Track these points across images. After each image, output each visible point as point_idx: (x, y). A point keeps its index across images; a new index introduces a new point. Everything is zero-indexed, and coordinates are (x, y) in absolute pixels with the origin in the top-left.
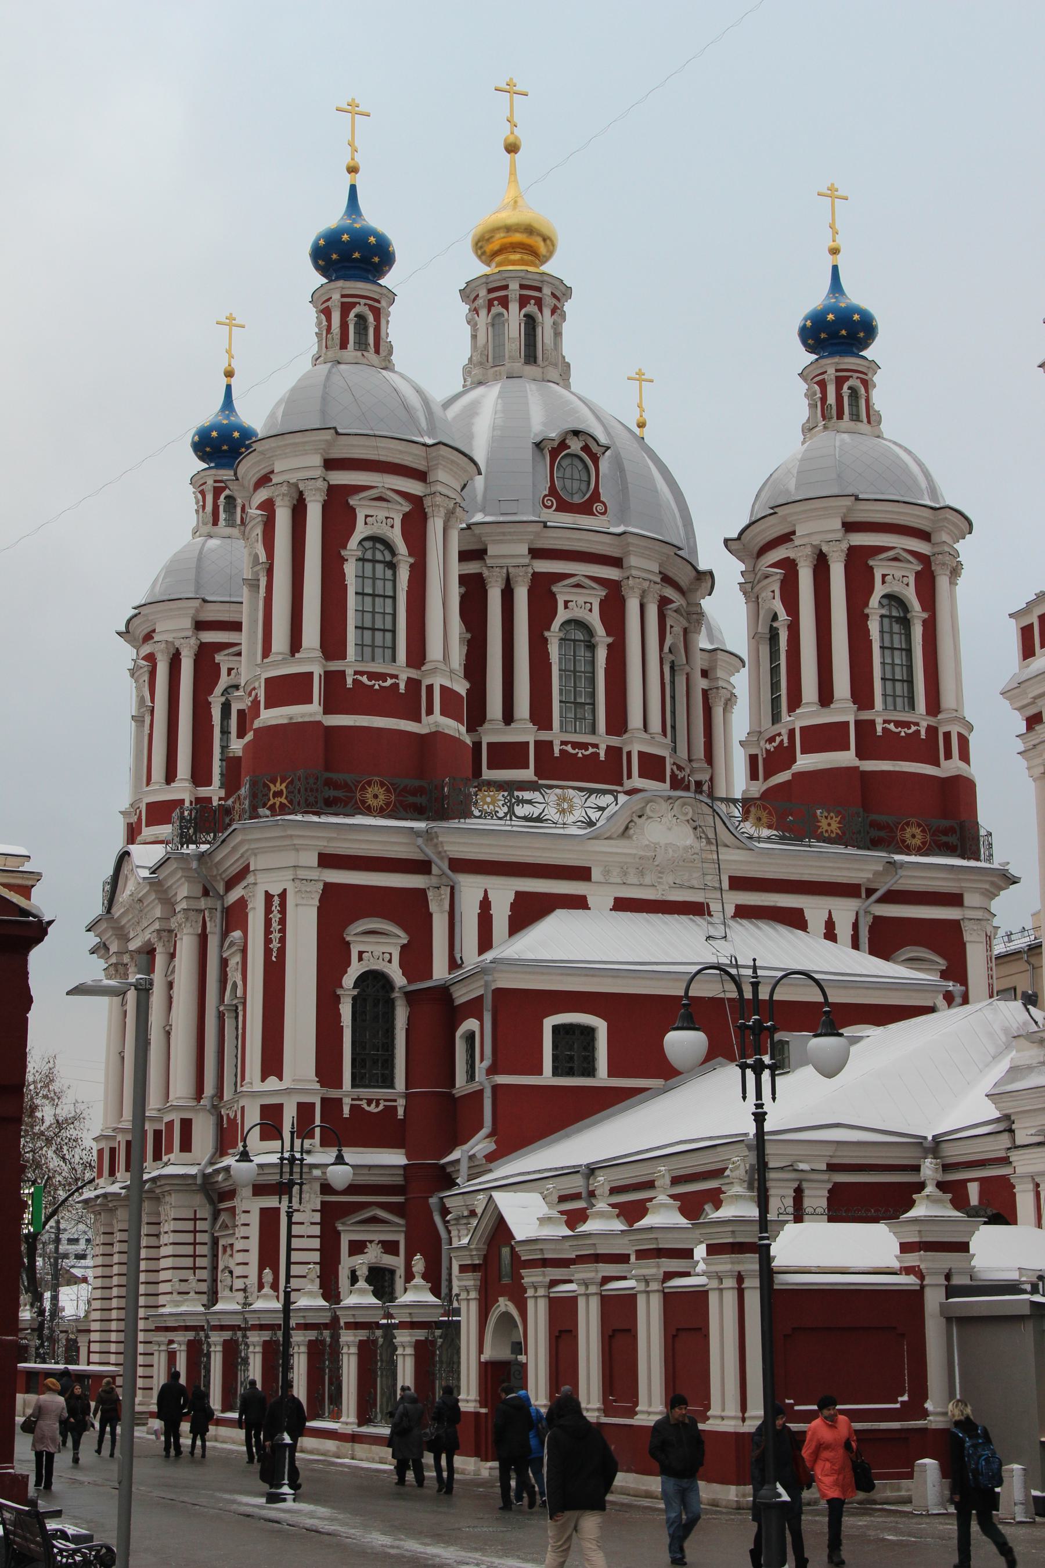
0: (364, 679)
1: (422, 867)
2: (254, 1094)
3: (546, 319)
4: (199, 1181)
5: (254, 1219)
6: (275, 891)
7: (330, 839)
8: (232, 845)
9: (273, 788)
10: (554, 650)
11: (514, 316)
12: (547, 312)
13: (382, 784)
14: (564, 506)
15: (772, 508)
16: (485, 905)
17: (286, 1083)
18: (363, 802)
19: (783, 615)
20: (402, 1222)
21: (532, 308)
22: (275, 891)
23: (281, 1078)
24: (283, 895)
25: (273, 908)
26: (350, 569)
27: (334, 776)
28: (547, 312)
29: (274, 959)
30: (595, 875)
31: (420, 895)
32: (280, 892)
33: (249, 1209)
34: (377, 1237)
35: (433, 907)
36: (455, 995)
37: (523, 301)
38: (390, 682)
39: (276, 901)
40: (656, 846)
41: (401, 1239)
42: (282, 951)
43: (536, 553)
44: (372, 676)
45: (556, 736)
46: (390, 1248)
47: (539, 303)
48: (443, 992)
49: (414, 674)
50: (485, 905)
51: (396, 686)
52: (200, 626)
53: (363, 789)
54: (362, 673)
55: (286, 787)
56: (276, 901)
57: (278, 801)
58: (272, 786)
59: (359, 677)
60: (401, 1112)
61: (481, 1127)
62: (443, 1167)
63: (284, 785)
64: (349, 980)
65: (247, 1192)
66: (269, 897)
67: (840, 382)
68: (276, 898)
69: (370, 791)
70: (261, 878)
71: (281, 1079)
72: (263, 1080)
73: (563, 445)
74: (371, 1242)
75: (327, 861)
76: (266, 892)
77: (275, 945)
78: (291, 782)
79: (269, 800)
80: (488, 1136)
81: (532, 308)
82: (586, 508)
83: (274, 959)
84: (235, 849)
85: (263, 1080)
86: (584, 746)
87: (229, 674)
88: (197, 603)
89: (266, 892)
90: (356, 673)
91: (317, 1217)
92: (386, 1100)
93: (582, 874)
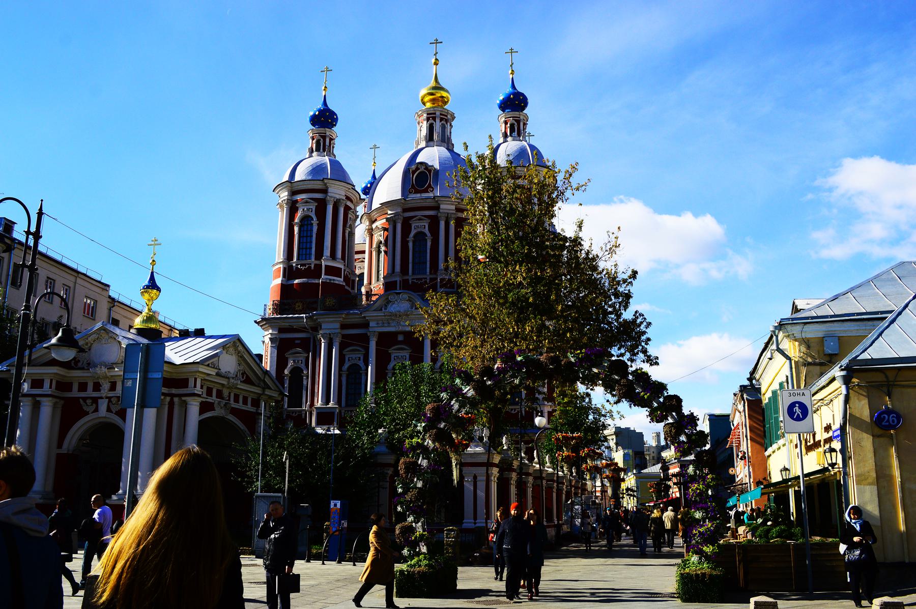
3: (438, 126)
10: (411, 245)
11: (425, 125)
12: (438, 120)
14: (417, 192)
21: (431, 121)
28: (438, 120)
37: (428, 119)
43: (405, 210)
45: (410, 277)
47: (434, 119)
49: (318, 262)
73: (417, 169)
81: (430, 121)
82: (426, 191)
86: (421, 279)
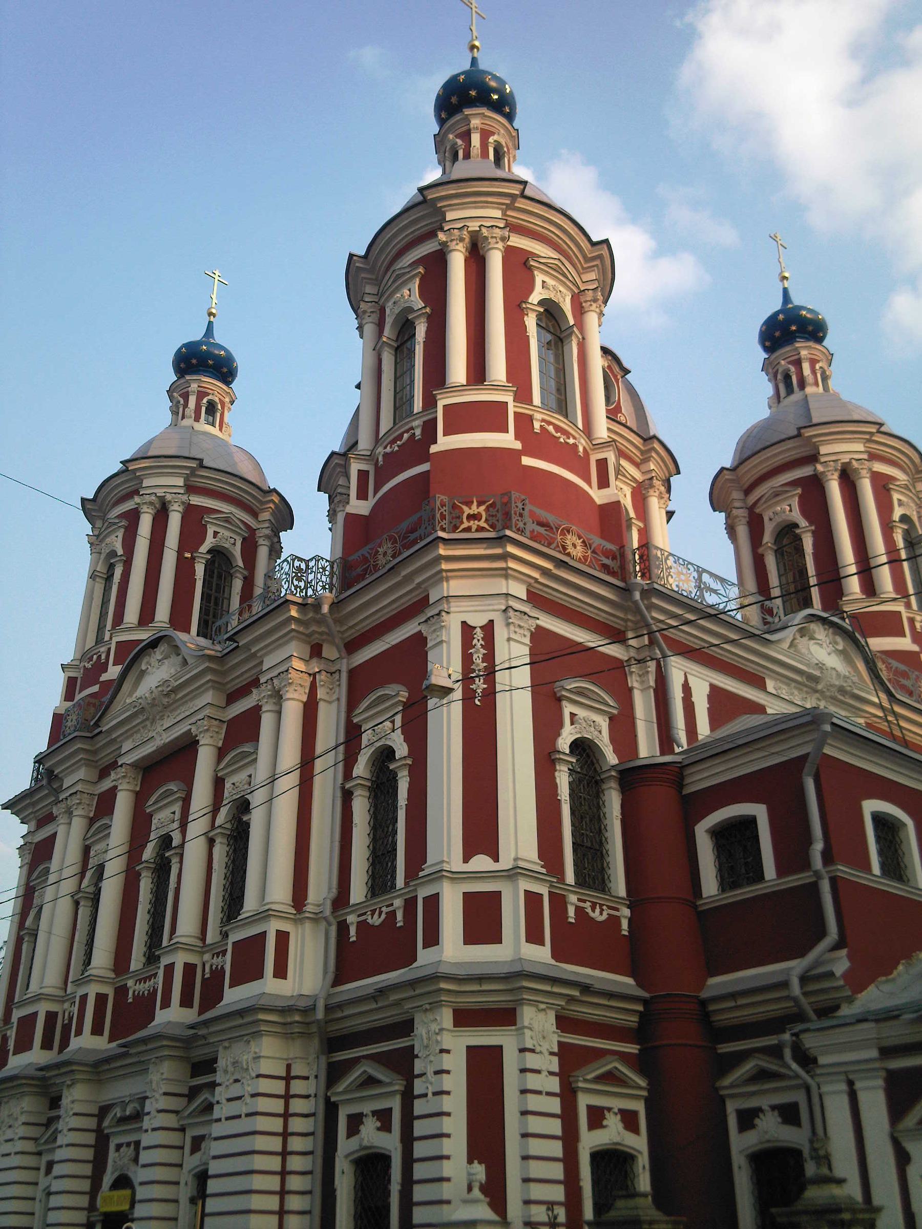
0: (551, 428)
1: (618, 637)
2: (457, 877)
4: (320, 1014)
5: (456, 1064)
6: (477, 620)
7: (545, 572)
8: (404, 573)
9: (467, 511)
13: (580, 537)
15: (799, 429)
16: (687, 689)
17: (506, 862)
18: (564, 548)
19: (803, 523)
20: (642, 1083)
22: (477, 620)
23: (496, 859)
24: (489, 628)
25: (475, 641)
26: (531, 322)
27: (538, 511)
29: (478, 703)
30: (770, 685)
31: (619, 667)
32: (484, 622)
33: (446, 1051)
34: (617, 1104)
35: (633, 681)
36: (688, 780)
38: (571, 441)
39: (479, 634)
40: (820, 666)
41: (639, 1107)
42: (490, 694)
44: (558, 428)
46: (629, 1120)
48: (672, 775)
50: (687, 689)
51: (575, 446)
52: (191, 489)
53: (563, 534)
54: (549, 423)
55: (487, 510)
56: (479, 634)
57: (474, 524)
58: (465, 508)
59: (546, 426)
60: (625, 924)
61: (822, 933)
62: (703, 1003)
63: (482, 508)
64: (564, 742)
65: (446, 1017)
66: (467, 629)
67: (813, 362)
68: (478, 630)
69: (570, 539)
70: (454, 606)
71: (496, 859)
72: (466, 860)
74: (609, 1109)
75: (535, 598)
76: (464, 623)
77: (480, 685)
78: (493, 505)
79: (462, 523)
80: (837, 947)
83: (478, 703)
84: (409, 578)
85: (466, 860)
87: (214, 537)
88: (194, 464)
89: (464, 623)
90: (543, 420)
91: (554, 1064)
92: (610, 908)
93: (758, 682)
